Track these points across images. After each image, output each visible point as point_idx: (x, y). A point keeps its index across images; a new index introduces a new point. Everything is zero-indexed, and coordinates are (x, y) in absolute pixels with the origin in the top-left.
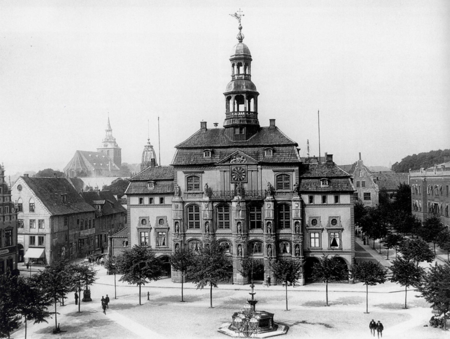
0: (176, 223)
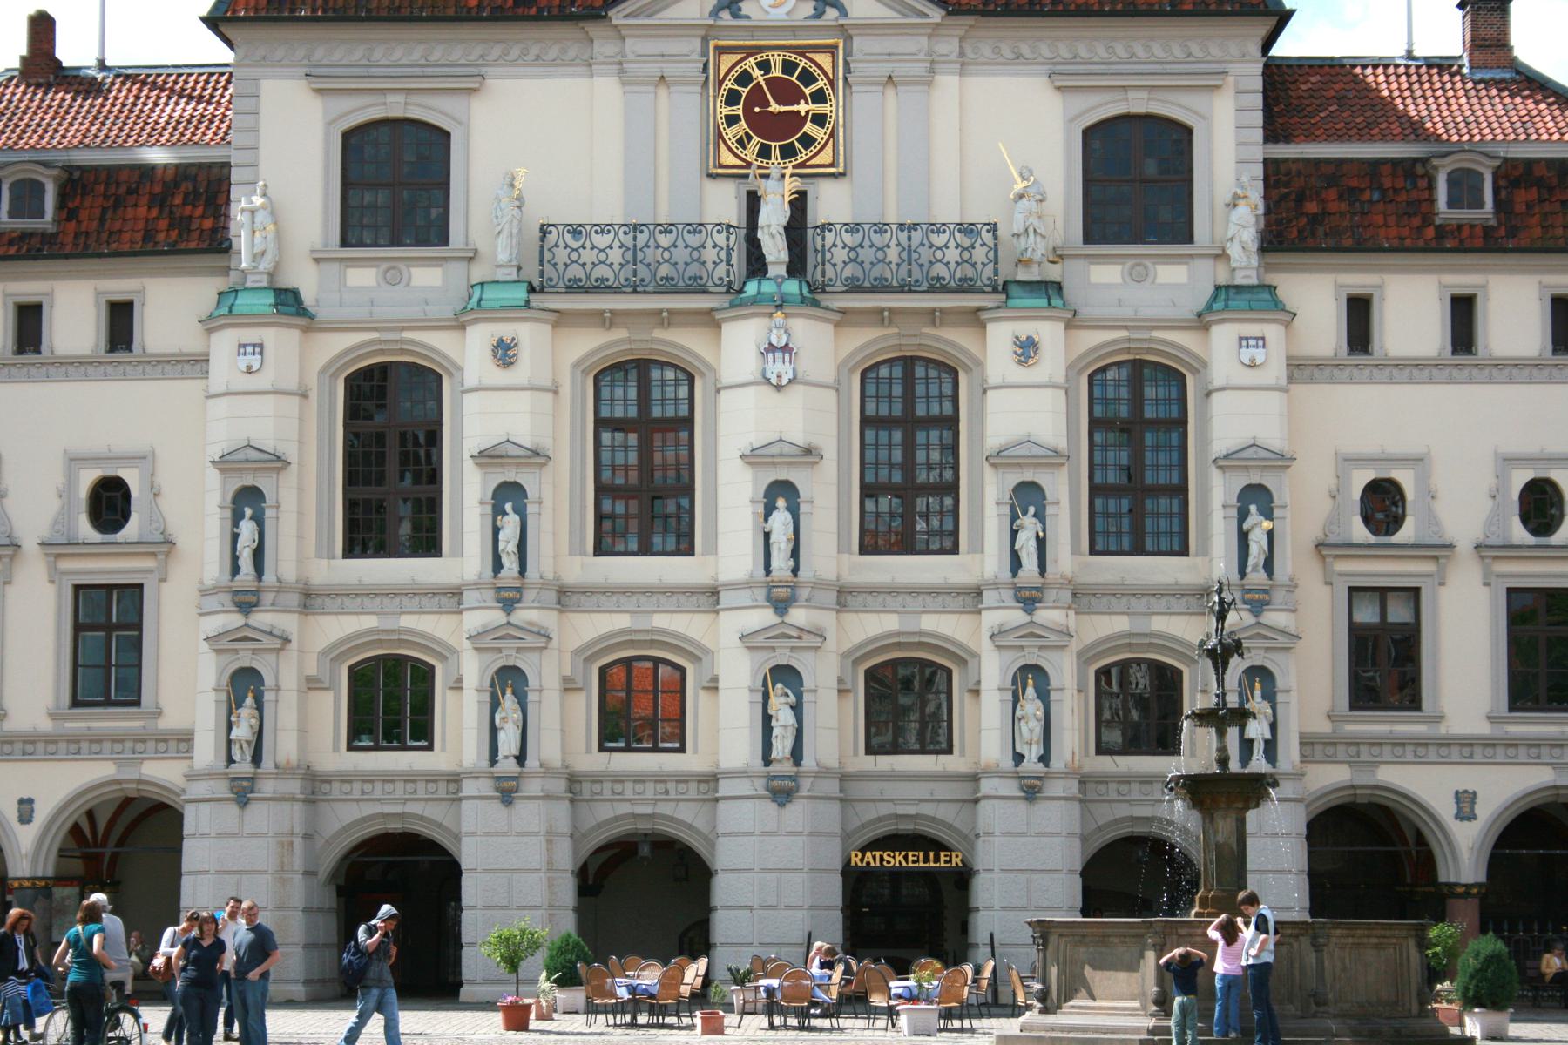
0: (247, 501)
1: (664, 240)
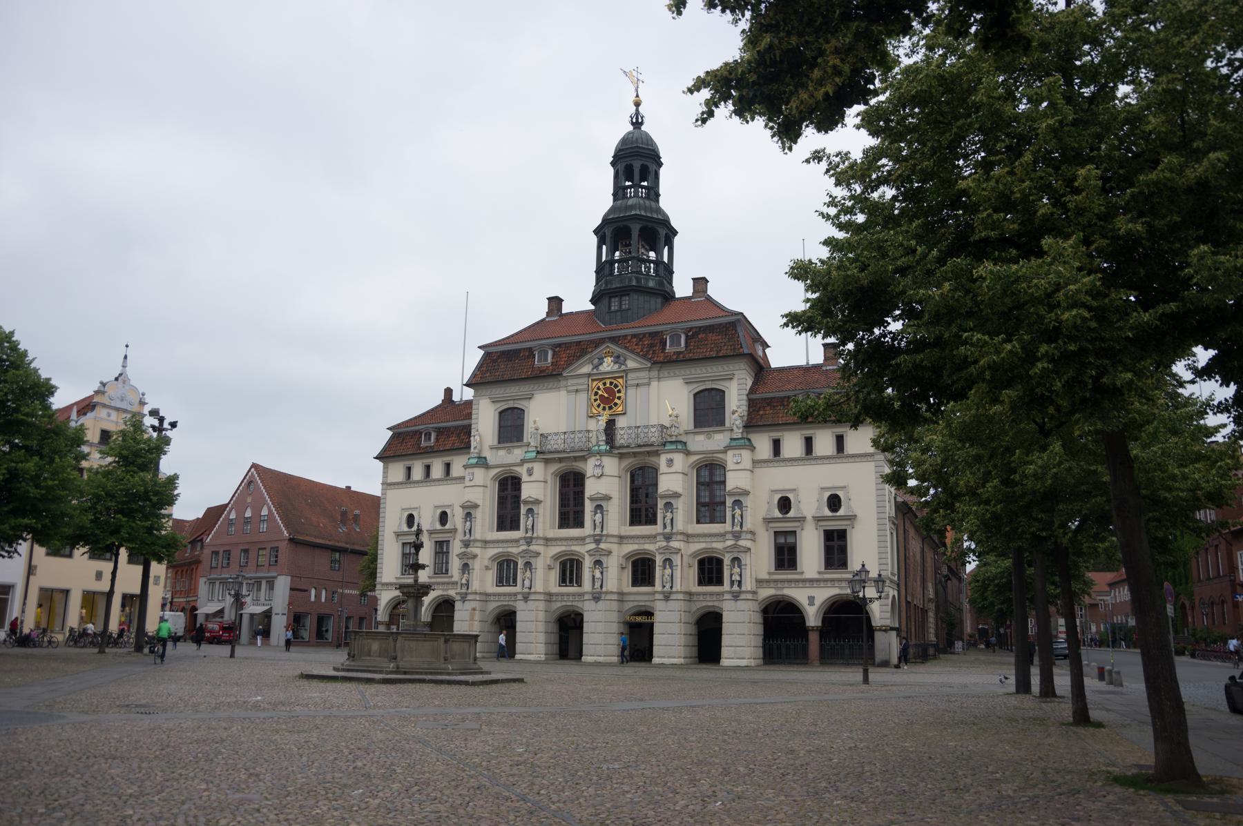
0: (468, 515)
1: (572, 436)
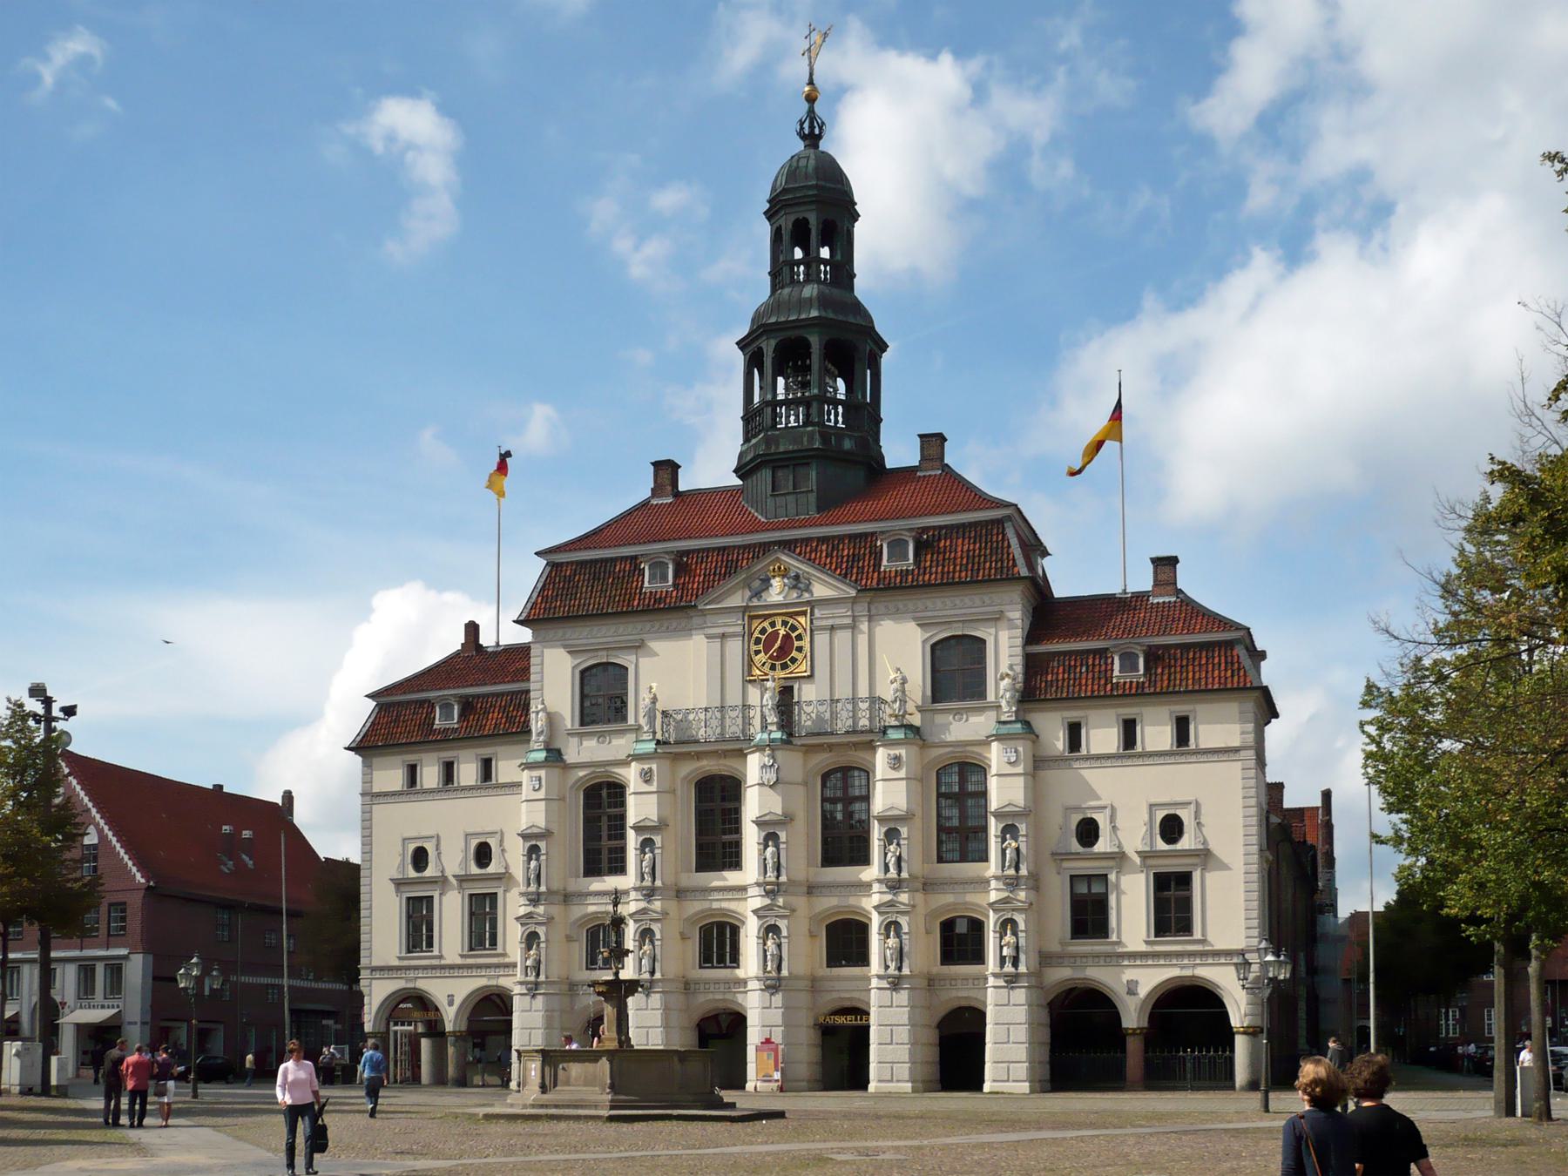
0: (533, 851)
